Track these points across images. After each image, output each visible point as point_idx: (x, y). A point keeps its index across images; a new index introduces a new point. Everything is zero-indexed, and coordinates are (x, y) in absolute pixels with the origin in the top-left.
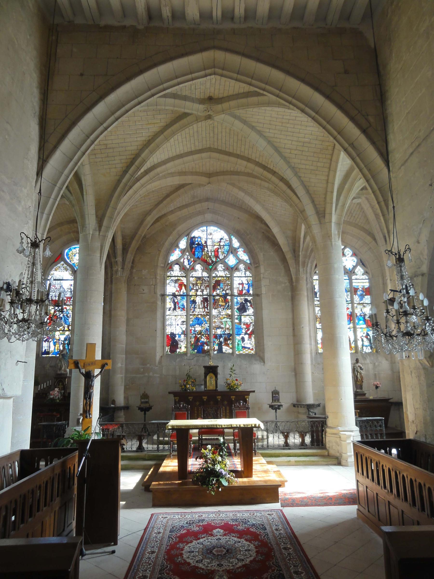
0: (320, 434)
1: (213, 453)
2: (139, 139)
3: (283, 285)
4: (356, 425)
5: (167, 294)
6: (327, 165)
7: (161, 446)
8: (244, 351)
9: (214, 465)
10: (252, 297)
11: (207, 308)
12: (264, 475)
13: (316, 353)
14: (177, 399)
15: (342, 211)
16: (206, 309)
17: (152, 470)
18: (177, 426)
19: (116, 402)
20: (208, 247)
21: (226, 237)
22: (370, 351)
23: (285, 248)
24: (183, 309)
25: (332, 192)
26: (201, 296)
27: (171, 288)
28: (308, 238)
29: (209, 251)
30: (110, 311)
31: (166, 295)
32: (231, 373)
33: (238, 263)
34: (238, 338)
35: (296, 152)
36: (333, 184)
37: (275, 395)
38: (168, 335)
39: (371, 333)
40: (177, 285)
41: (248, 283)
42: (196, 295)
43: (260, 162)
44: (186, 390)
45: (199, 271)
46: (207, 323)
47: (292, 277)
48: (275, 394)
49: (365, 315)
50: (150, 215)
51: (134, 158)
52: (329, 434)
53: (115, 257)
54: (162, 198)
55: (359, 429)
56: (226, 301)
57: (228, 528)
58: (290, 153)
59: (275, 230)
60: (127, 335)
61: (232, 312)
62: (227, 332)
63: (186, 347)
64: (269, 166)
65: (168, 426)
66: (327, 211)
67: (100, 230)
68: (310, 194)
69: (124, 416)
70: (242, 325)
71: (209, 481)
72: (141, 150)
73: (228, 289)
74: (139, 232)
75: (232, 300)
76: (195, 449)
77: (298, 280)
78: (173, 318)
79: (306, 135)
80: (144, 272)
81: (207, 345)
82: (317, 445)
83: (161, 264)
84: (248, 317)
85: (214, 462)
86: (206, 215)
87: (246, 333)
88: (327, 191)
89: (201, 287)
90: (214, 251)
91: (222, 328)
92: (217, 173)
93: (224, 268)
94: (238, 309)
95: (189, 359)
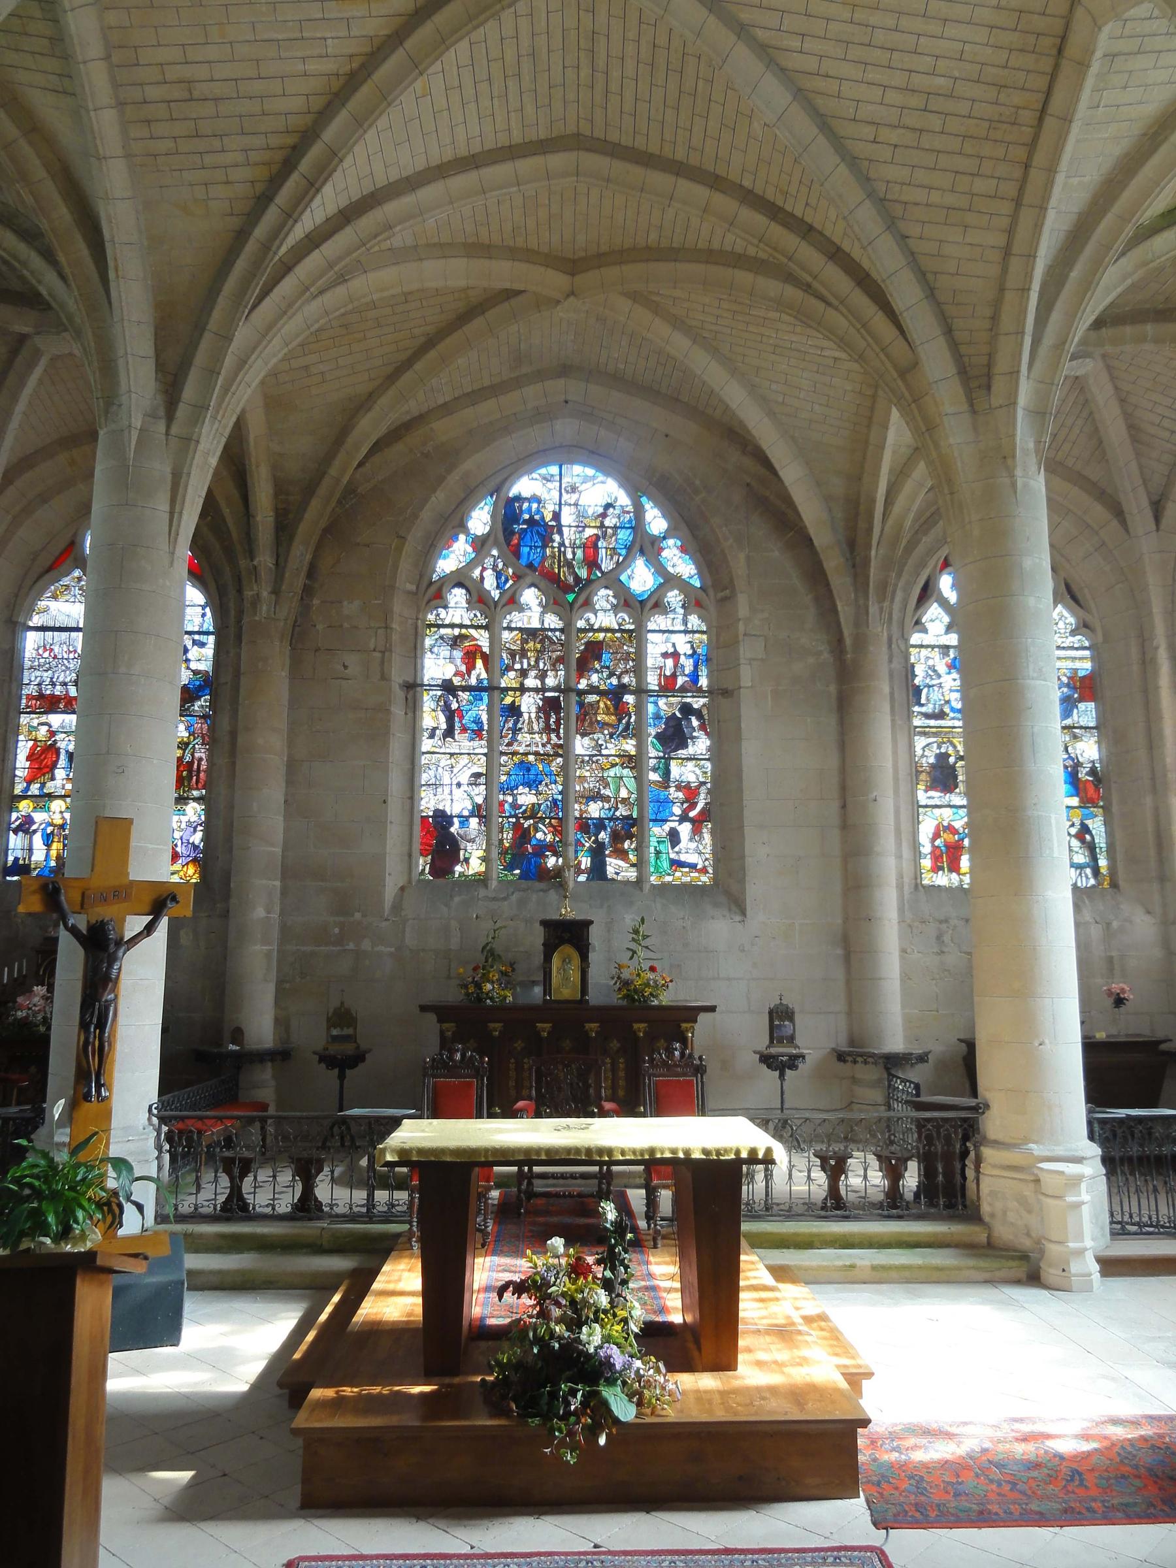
0: (958, 1166)
2: (312, 67)
3: (811, 660)
4: (1091, 1137)
5: (426, 682)
6: (1010, 189)
7: (381, 1196)
8: (678, 874)
9: (576, 1323)
10: (705, 700)
11: (557, 731)
12: (779, 1353)
13: (916, 886)
15: (1055, 365)
16: (553, 736)
17: (336, 1298)
18: (421, 1151)
19: (246, 1035)
20: (565, 530)
21: (624, 500)
22: (1092, 882)
23: (822, 536)
24: (478, 733)
25: (1025, 290)
26: (536, 690)
27: (438, 665)
28: (920, 470)
29: (567, 543)
30: (233, 734)
31: (423, 685)
32: (633, 946)
33: (661, 585)
34: (658, 831)
35: (894, 136)
36: (1031, 257)
39: (1097, 826)
40: (458, 654)
41: (695, 652)
42: (523, 689)
43: (758, 190)
44: (479, 1000)
45: (532, 609)
46: (555, 782)
47: (841, 632)
48: (781, 1019)
49: (1077, 765)
50: (369, 409)
51: (294, 148)
52: (994, 1166)
53: (251, 555)
54: (410, 352)
55: (1099, 1151)
56: (620, 710)
58: (874, 142)
59: (792, 474)
60: (287, 816)
61: (640, 746)
62: (622, 811)
63: (484, 859)
64: (788, 208)
65: (383, 1151)
66: (1002, 365)
67: (170, 417)
68: (938, 304)
69: (273, 1083)
70: (672, 790)
71: (553, 1395)
72: (320, 113)
73: (627, 672)
74: (333, 472)
75: (640, 707)
76: (505, 1211)
77: (861, 642)
78: (445, 761)
79: (941, 63)
80: (351, 608)
81: (556, 854)
82: (947, 1207)
83: (405, 582)
84: (691, 764)
86: (559, 425)
87: (684, 818)
88: (1002, 290)
89: (537, 662)
90: (584, 546)
91: (606, 799)
92: (600, 255)
93: (615, 602)
94: (658, 736)
95: (494, 899)
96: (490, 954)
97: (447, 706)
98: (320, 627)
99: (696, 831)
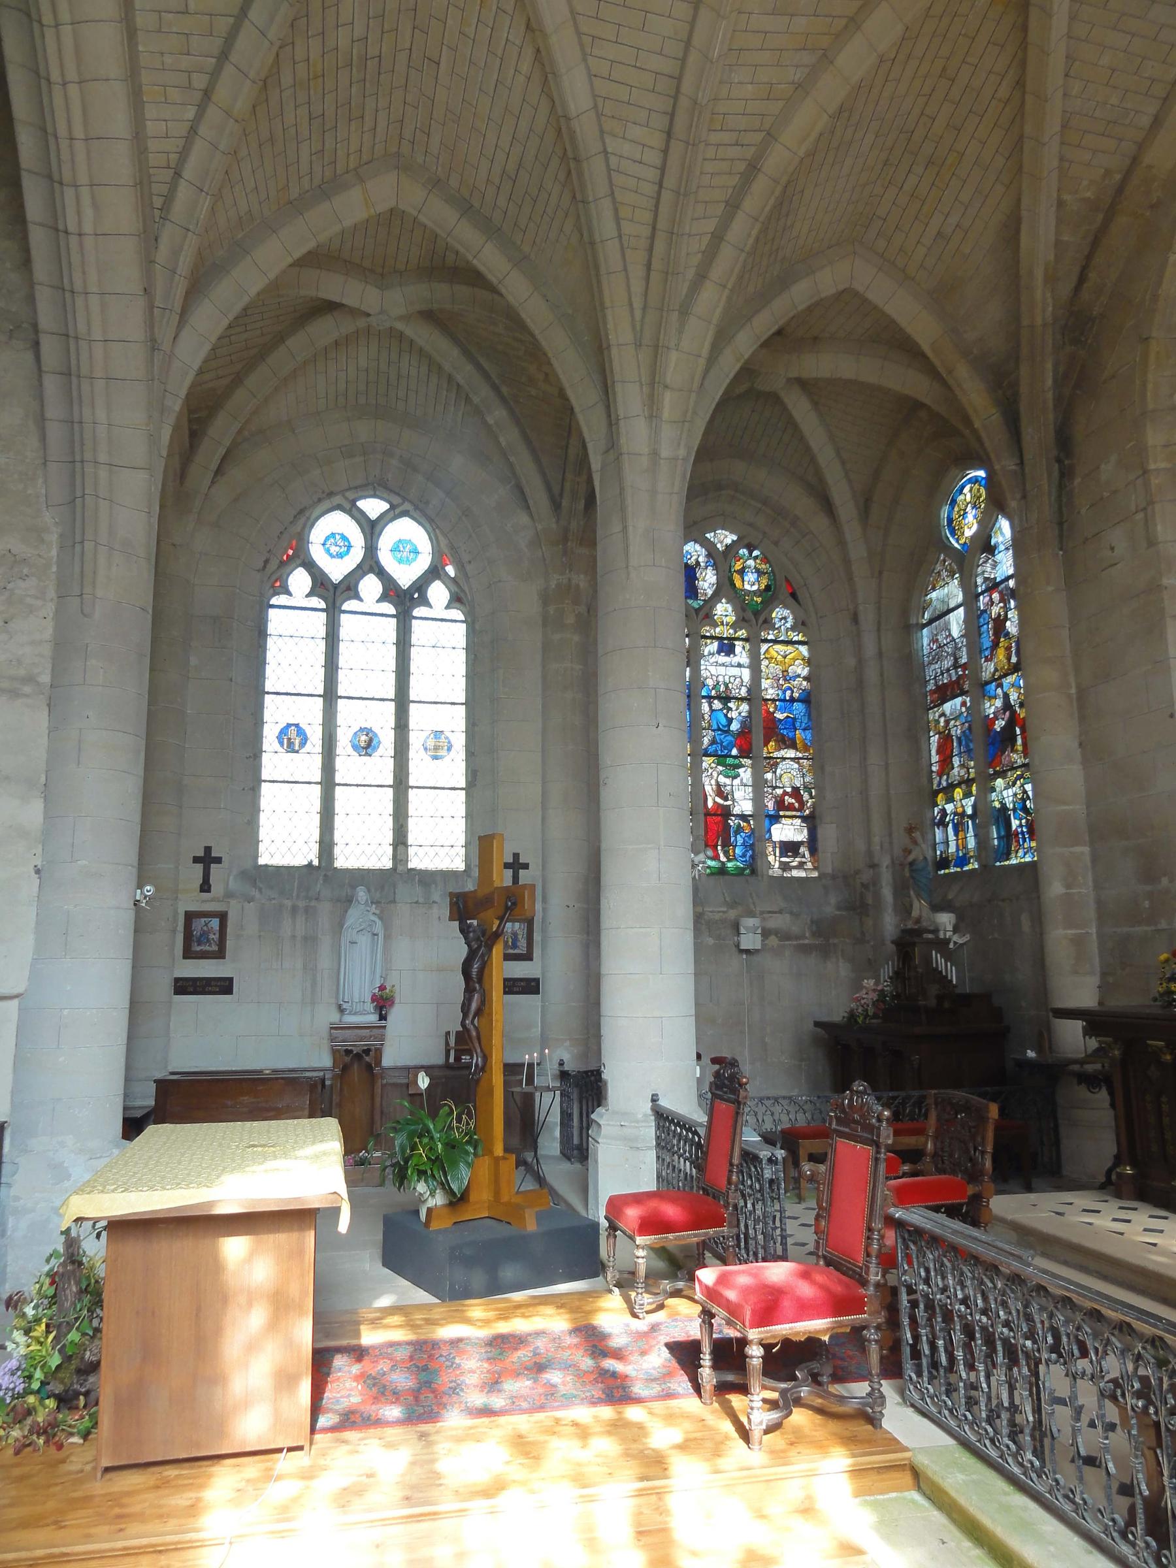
74: (1025, 322)
80: (1108, 470)
98: (1083, 511)
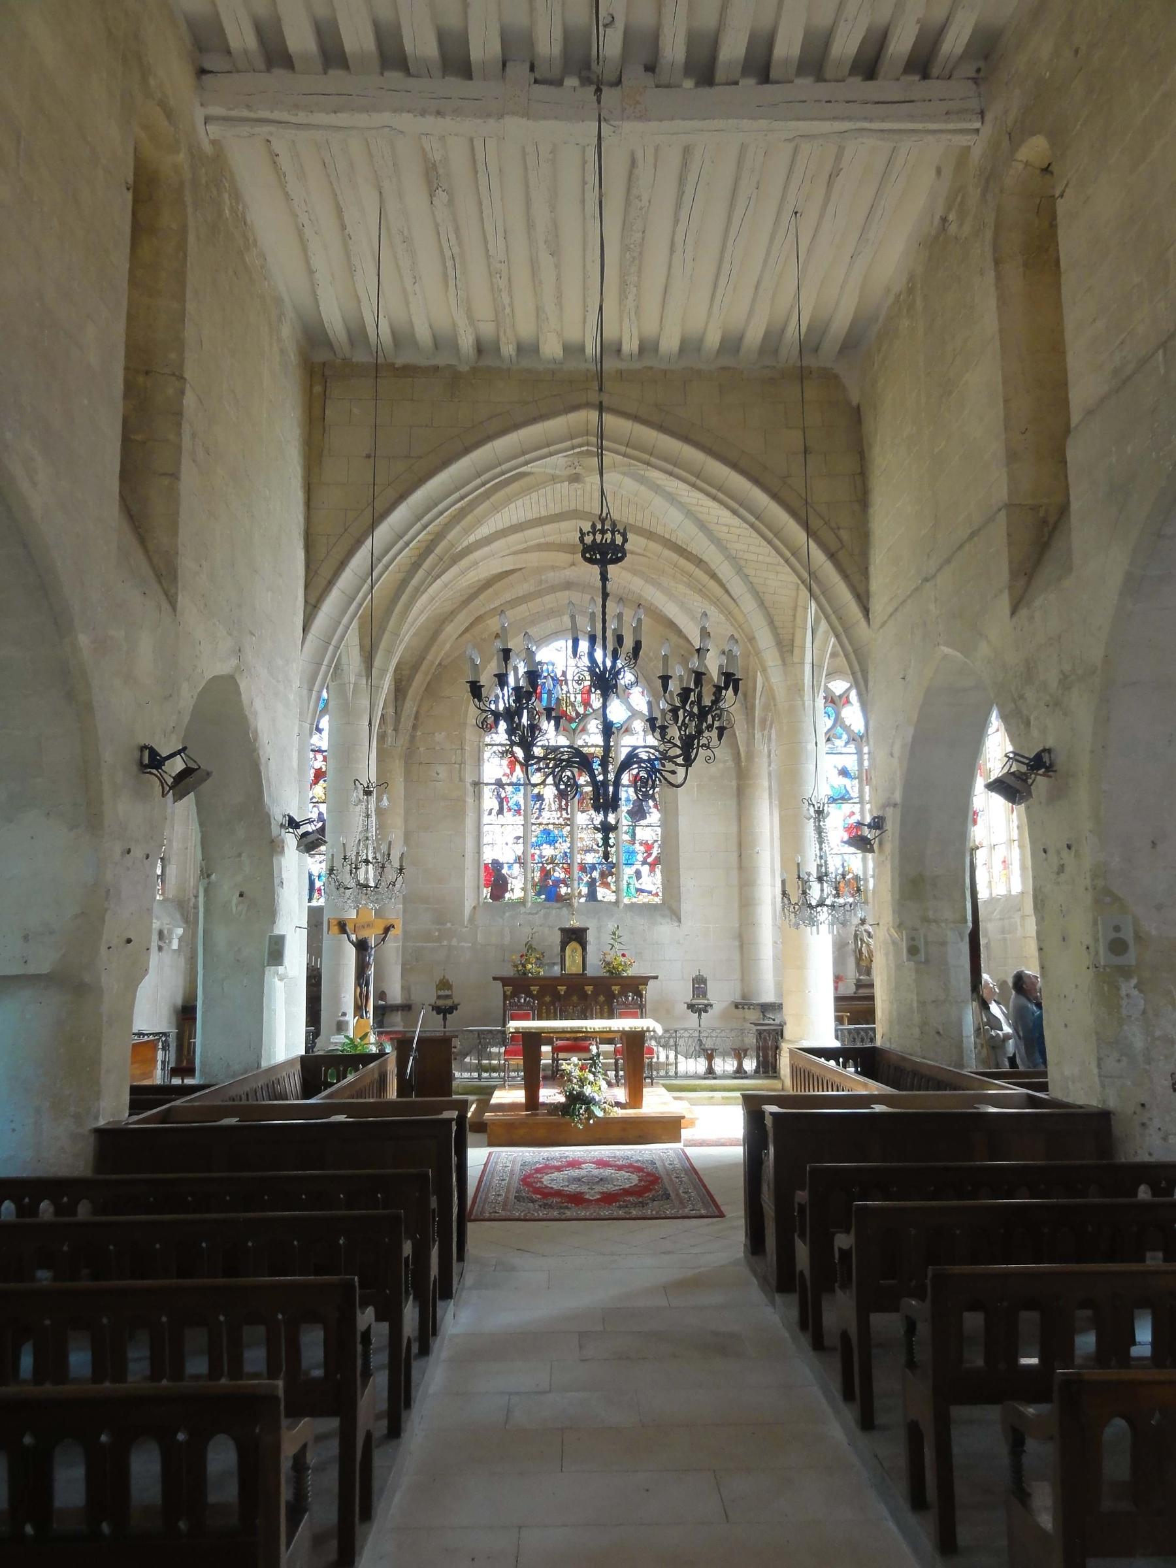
1: (582, 1069)
3: (721, 765)
4: (837, 1038)
8: (641, 897)
11: (566, 809)
14: (509, 989)
20: (570, 683)
24: (518, 812)
32: (612, 942)
33: (630, 718)
34: (628, 871)
37: (699, 985)
38: (486, 866)
43: (673, 539)
57: (601, 1163)
66: (797, 643)
74: (429, 657)
77: (750, 756)
80: (440, 737)
81: (566, 885)
85: (582, 1082)
87: (644, 863)
94: (628, 812)
96: (530, 948)
97: (499, 795)
98: (422, 749)
99: (652, 870)
